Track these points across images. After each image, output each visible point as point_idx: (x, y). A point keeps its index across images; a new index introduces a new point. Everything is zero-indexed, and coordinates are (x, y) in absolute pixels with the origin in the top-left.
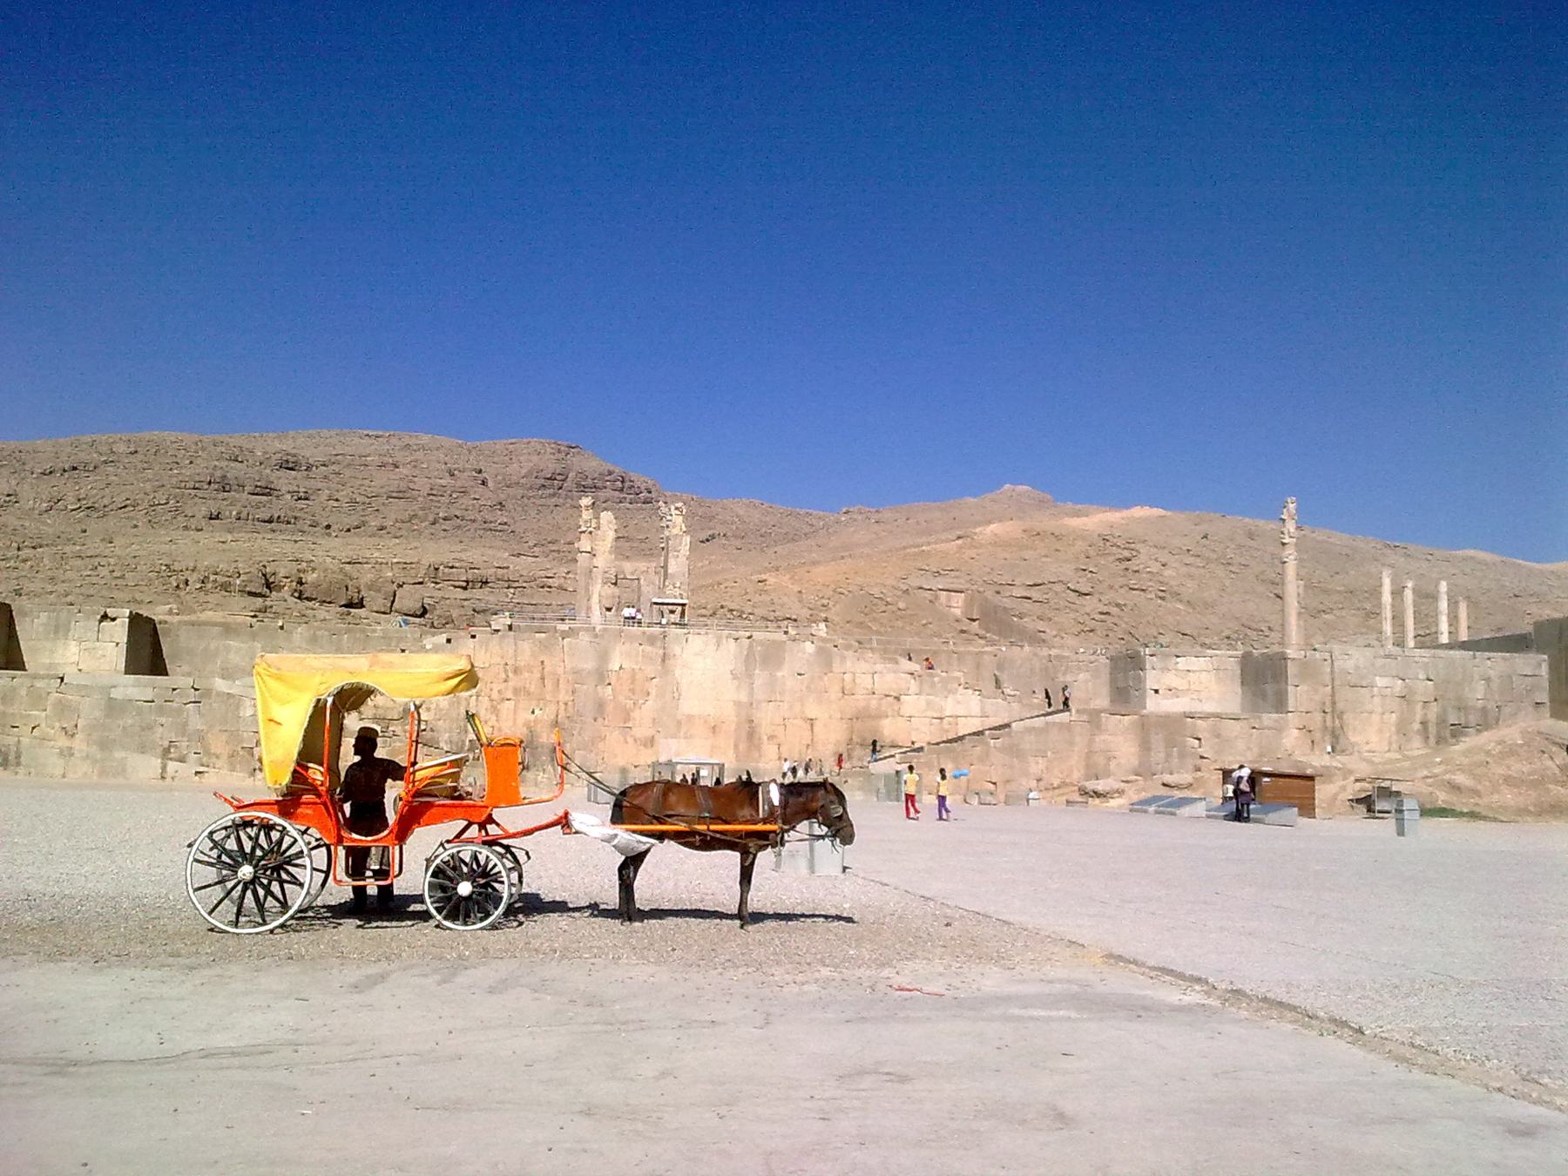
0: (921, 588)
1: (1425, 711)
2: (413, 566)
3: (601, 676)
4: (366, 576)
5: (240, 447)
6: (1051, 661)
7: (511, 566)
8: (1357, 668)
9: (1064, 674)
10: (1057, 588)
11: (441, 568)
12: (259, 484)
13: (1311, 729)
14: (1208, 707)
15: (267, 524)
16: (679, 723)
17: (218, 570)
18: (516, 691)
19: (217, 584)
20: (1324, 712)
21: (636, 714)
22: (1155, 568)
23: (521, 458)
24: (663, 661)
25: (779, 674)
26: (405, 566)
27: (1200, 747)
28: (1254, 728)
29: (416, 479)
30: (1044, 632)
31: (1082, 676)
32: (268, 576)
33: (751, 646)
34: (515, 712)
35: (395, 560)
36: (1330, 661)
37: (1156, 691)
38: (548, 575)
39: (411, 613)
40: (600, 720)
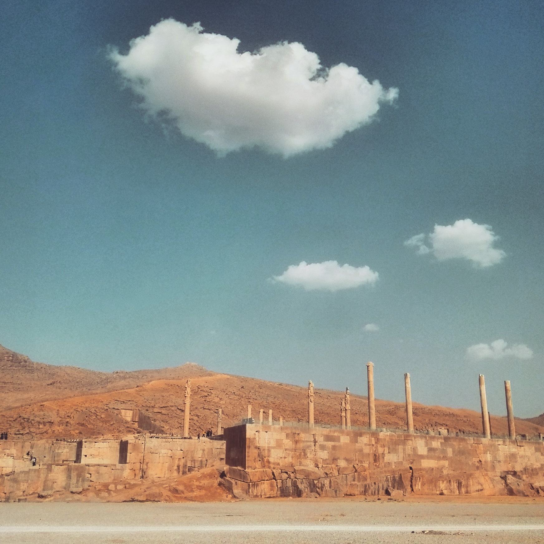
0: (114, 408)
1: (179, 462)
6: (53, 445)
8: (154, 446)
9: (59, 449)
10: (173, 408)
13: (135, 469)
14: (106, 462)
20: (140, 463)
22: (217, 400)
27: (91, 477)
28: (112, 469)
30: (163, 427)
31: (65, 451)
36: (144, 444)
37: (86, 456)
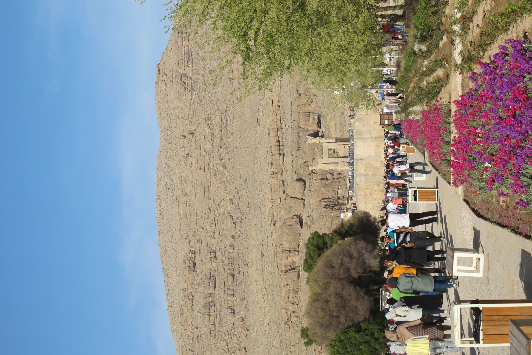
2: (273, 187)
3: (366, 175)
4: (283, 214)
5: (182, 298)
7: (267, 126)
11: (272, 170)
12: (208, 284)
15: (235, 276)
16: (377, 155)
17: (286, 296)
18: (371, 195)
19: (294, 296)
21: (375, 166)
23: (171, 107)
24: (362, 160)
25: (364, 131)
26: (273, 192)
29: (194, 180)
32: (287, 269)
33: (357, 138)
34: (376, 195)
35: (270, 198)
38: (271, 103)
39: (303, 187)
40: (377, 175)
